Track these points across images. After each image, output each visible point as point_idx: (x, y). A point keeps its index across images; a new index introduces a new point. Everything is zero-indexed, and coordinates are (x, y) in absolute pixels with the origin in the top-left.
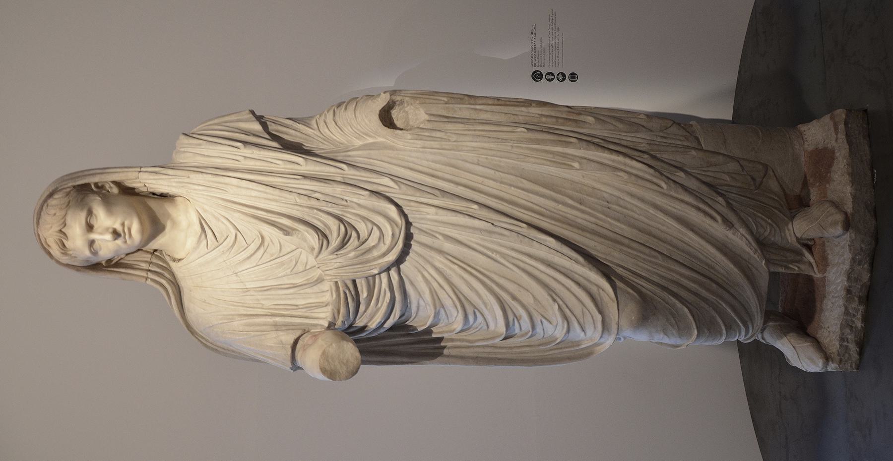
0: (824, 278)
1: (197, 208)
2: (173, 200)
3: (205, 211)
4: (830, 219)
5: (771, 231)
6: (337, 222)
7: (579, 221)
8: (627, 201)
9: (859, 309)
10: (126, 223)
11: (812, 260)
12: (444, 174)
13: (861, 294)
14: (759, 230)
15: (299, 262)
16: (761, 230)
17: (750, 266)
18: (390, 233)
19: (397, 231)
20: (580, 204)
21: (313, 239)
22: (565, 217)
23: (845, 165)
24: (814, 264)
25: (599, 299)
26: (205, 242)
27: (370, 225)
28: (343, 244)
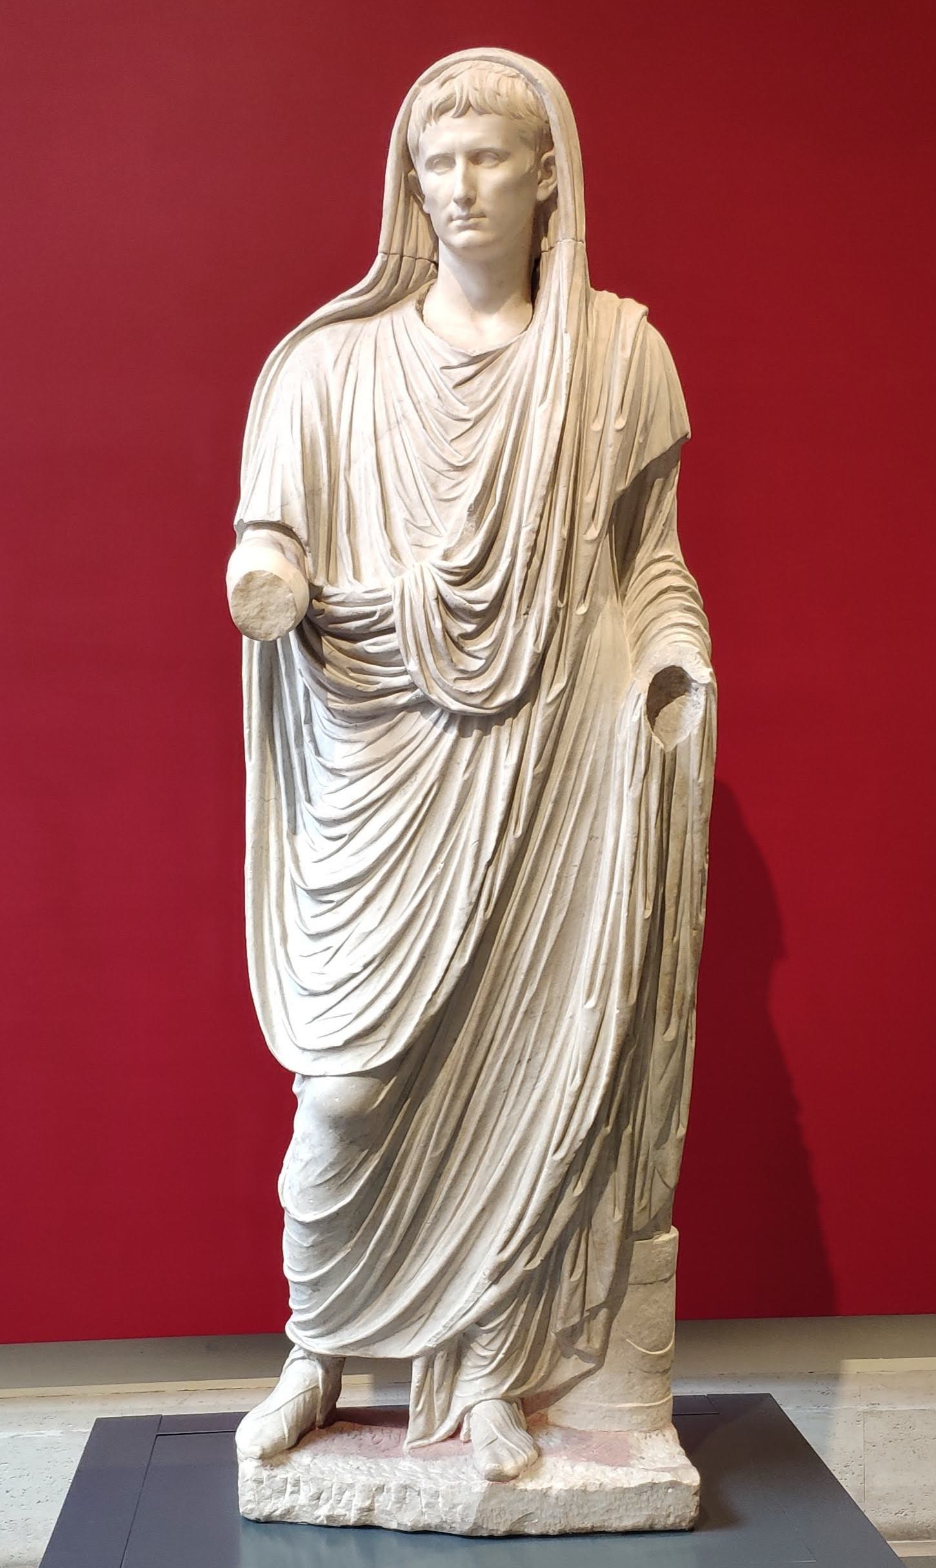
0: (403, 1456)
1: (513, 346)
2: (528, 302)
3: (509, 362)
4: (504, 1453)
5: (484, 1357)
6: (490, 598)
7: (497, 1011)
8: (531, 1094)
9: (349, 1510)
10: (485, 221)
11: (433, 1439)
12: (573, 780)
13: (376, 1511)
14: (485, 1335)
15: (422, 532)
16: (484, 1339)
17: (423, 1320)
18: (473, 690)
19: (477, 700)
20: (526, 1012)
21: (465, 557)
22: (503, 986)
23: (599, 1480)
24: (426, 1442)
25: (367, 1042)
26: (455, 362)
27: (485, 654)
28: (450, 610)
